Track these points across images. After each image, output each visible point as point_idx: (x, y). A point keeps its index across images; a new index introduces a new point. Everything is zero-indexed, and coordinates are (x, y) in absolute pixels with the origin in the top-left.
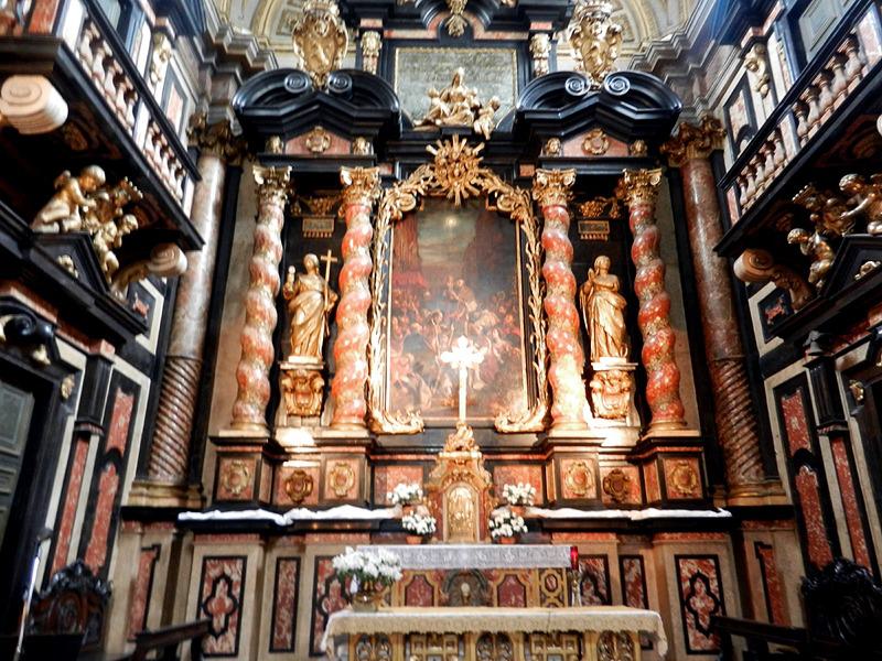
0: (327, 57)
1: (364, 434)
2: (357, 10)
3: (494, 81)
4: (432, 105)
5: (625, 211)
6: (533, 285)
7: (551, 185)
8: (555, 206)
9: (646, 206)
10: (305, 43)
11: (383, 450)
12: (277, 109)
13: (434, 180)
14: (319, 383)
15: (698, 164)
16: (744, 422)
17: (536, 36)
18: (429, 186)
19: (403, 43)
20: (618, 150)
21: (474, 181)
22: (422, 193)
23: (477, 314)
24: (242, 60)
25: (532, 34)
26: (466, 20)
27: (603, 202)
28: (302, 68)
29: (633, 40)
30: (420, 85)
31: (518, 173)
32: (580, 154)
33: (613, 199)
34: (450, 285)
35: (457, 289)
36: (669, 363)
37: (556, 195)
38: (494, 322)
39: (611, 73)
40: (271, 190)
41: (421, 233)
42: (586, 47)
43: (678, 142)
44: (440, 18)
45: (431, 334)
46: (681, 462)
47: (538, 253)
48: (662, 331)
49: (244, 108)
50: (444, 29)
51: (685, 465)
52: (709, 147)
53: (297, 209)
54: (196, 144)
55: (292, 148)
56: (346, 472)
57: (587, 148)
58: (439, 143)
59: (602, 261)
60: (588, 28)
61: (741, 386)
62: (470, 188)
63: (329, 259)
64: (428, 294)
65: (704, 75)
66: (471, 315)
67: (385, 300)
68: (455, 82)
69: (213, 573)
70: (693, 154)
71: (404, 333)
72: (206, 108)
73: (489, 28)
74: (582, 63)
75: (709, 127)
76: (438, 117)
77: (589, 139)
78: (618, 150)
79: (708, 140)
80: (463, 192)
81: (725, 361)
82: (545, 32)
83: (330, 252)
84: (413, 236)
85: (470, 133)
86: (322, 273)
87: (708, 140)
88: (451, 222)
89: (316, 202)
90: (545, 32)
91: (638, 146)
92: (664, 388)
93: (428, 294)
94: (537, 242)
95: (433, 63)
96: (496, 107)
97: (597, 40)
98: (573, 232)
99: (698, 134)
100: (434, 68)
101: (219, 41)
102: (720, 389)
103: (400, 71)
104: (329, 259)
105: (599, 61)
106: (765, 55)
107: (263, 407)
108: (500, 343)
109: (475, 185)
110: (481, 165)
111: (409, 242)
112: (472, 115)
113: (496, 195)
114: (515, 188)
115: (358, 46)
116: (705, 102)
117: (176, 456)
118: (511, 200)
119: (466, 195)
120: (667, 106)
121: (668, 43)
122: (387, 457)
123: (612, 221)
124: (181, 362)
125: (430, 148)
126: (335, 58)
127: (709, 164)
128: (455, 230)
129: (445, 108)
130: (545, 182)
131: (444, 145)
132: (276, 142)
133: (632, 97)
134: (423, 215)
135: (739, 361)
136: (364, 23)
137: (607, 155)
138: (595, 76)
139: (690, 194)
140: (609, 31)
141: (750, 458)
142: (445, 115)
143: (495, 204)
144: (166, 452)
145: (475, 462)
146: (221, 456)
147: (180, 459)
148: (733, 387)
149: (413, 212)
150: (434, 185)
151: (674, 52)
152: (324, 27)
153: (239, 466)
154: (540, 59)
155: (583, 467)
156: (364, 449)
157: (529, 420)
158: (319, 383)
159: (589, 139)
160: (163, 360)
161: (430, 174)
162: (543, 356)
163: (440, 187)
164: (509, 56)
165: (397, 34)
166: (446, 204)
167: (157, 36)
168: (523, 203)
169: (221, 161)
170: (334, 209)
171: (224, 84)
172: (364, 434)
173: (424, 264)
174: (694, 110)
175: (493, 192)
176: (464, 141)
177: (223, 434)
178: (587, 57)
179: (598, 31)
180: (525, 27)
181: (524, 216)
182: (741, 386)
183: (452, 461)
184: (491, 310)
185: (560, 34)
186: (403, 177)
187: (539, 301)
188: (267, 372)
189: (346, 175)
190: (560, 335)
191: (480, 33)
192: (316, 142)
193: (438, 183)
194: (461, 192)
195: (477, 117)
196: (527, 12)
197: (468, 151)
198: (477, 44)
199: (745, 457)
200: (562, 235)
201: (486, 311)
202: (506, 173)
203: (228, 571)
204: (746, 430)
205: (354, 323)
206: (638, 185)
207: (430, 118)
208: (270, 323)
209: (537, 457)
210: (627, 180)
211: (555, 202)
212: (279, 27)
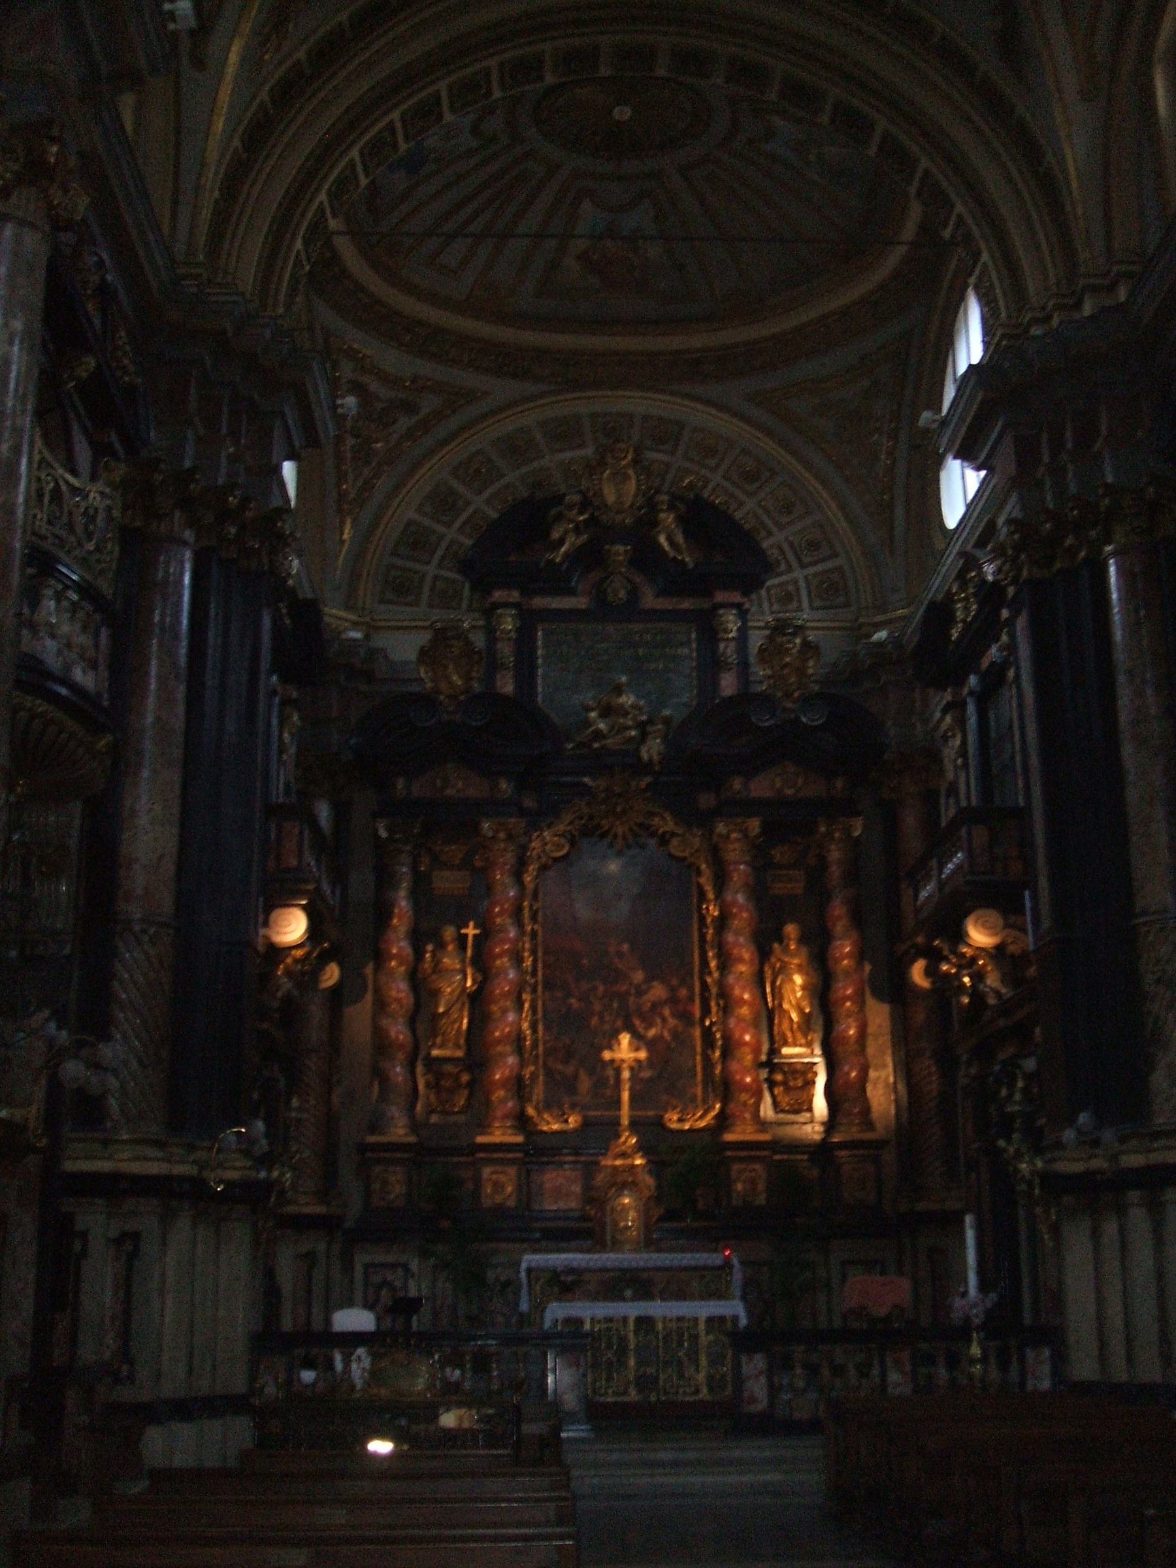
1: (520, 1139)
4: (587, 723)
14: (465, 1078)
17: (721, 611)
21: (640, 820)
26: (629, 581)
29: (849, 606)
34: (612, 949)
35: (620, 955)
56: (502, 1178)
62: (635, 828)
63: (471, 931)
66: (638, 987)
67: (534, 973)
68: (618, 690)
69: (376, 1279)
82: (732, 605)
90: (732, 605)
91: (839, 784)
98: (758, 892)
108: (672, 1022)
113: (668, 836)
132: (401, 783)
136: (498, 595)
155: (753, 1174)
157: (702, 1117)
165: (539, 602)
185: (754, 596)
201: (655, 983)
203: (390, 1278)
206: (837, 835)
211: (736, 853)
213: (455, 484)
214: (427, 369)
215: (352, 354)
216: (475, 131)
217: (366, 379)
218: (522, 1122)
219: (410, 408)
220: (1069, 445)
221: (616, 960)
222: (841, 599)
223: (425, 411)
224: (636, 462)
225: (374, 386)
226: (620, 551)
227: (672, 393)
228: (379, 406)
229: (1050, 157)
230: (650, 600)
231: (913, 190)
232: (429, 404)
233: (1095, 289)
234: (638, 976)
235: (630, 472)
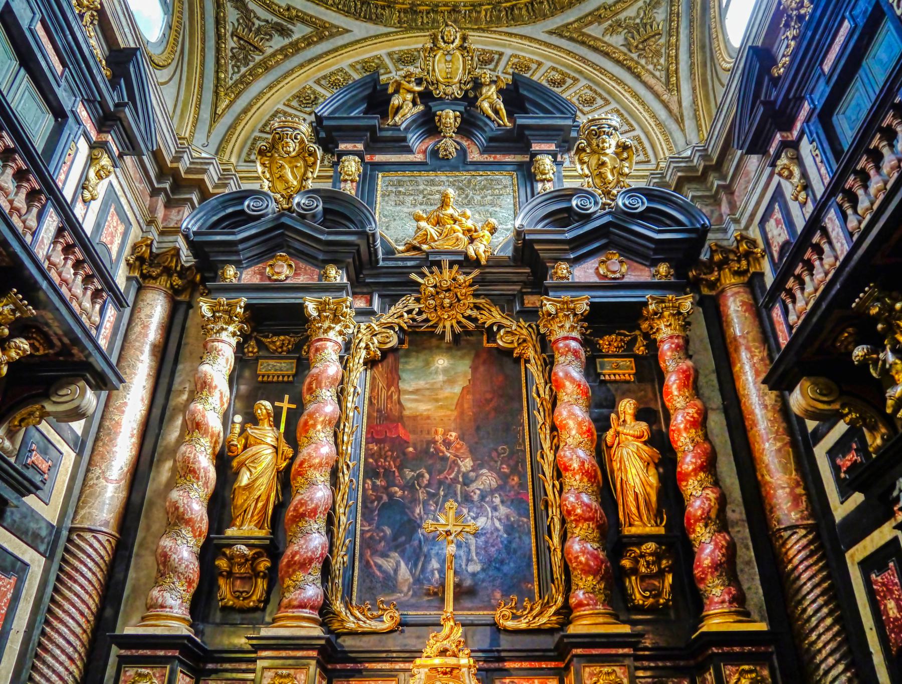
0: (295, 177)
1: (317, 631)
2: (334, 134)
3: (493, 204)
4: (419, 228)
5: (653, 345)
6: (542, 436)
7: (561, 314)
8: (566, 338)
9: (678, 337)
10: (270, 163)
11: (345, 656)
12: (233, 234)
13: (420, 313)
14: (264, 564)
15: (735, 290)
16: (825, 610)
17: (539, 157)
18: (414, 320)
19: (386, 167)
20: (643, 275)
21: (469, 312)
22: (405, 326)
23: (472, 474)
24: (200, 186)
25: (534, 155)
26: (458, 143)
27: (626, 336)
28: (266, 189)
30: (406, 210)
31: (522, 303)
32: (594, 279)
33: (637, 332)
34: (439, 438)
35: (447, 444)
36: (719, 532)
37: (567, 325)
38: (494, 484)
39: (624, 190)
40: (221, 324)
41: (404, 375)
42: (594, 161)
43: (710, 266)
44: (430, 144)
45: (415, 500)
46: (746, 667)
47: (547, 397)
48: (708, 491)
49: (195, 233)
50: (435, 153)
51: (750, 671)
52: (747, 271)
53: (252, 348)
54: (137, 274)
55: (249, 276)
57: (602, 272)
58: (425, 270)
59: (627, 406)
60: (594, 142)
61: (815, 563)
62: (464, 320)
63: (285, 405)
64: (411, 449)
65: (732, 193)
66: (465, 476)
70: (728, 279)
71: (379, 499)
72: (154, 235)
73: (485, 150)
74: (590, 180)
75: (744, 247)
76: (425, 242)
77: (603, 262)
78: (643, 275)
79: (744, 263)
80: (455, 325)
81: (793, 528)
82: (547, 153)
83: (287, 397)
84: (393, 379)
85: (461, 258)
86: (277, 425)
87: (744, 263)
88: (442, 362)
89: (275, 339)
90: (547, 153)
91: (663, 268)
92: (716, 566)
93: (411, 449)
94: (546, 383)
95: (421, 187)
96: (493, 231)
97: (605, 155)
98: (590, 369)
99: (732, 256)
100: (423, 191)
101: (175, 165)
102: (790, 567)
103: (383, 196)
104: (285, 405)
105: (610, 177)
106: (798, 160)
107: (188, 596)
108: (503, 510)
109: (469, 318)
110: (476, 296)
111: (389, 387)
112: (466, 239)
113: (495, 329)
114: (518, 321)
115: (335, 172)
116: (737, 221)
117: (67, 663)
118: (513, 334)
119: (458, 329)
120: (692, 224)
121: (689, 159)
122: (350, 666)
123: (636, 357)
124: (88, 536)
125: (414, 276)
126: (304, 178)
127: (748, 290)
128: (445, 371)
129: (432, 231)
130: (553, 310)
131: (432, 273)
132: (231, 271)
133: (647, 216)
134: (407, 354)
135: (810, 529)
137: (626, 280)
138: (607, 193)
139: (729, 324)
140: (618, 146)
141: (837, 662)
142: (432, 237)
143: (495, 341)
144: (54, 657)
145: (464, 670)
146: (123, 661)
147: (73, 668)
148: (806, 563)
149: (393, 350)
150: (419, 318)
151: (694, 169)
152: (293, 147)
153: (145, 676)
154: (543, 181)
155: (613, 677)
156: (314, 654)
157: (540, 613)
158: (264, 564)
159: (603, 262)
160: (65, 533)
161: (416, 307)
162: (558, 527)
163: (427, 320)
164: (506, 180)
165: (379, 158)
166: (434, 342)
167: (96, 152)
168: (529, 338)
169: (166, 293)
170: (298, 347)
171: (179, 211)
172: (317, 631)
173: (406, 413)
174: (725, 231)
175: (492, 326)
176: (456, 267)
177: (129, 631)
178: (596, 172)
179: (606, 145)
180: (525, 148)
181: (531, 353)
182: (815, 563)
183: (434, 669)
184: (491, 469)
185: (566, 156)
186: (383, 310)
187: (550, 456)
188: (197, 549)
189: (311, 308)
190: (578, 498)
191: (474, 155)
192: (277, 270)
193: (424, 316)
194: (452, 326)
195: (472, 240)
196: (527, 133)
197: (461, 278)
198: (471, 167)
199: (831, 661)
200: (576, 373)
201: (484, 471)
202: (505, 303)
204: (829, 621)
205: (313, 484)
206: (666, 313)
207: (415, 243)
208: (206, 484)
209: (552, 665)
210: (652, 307)
212: (249, 155)
213: (319, 89)
218: (325, 612)
219: (284, 32)
221: (443, 448)
222: (642, 158)
223: (295, 37)
224: (462, 48)
226: (449, 117)
230: (474, 155)
232: (300, 31)
234: (467, 464)
235: (458, 53)
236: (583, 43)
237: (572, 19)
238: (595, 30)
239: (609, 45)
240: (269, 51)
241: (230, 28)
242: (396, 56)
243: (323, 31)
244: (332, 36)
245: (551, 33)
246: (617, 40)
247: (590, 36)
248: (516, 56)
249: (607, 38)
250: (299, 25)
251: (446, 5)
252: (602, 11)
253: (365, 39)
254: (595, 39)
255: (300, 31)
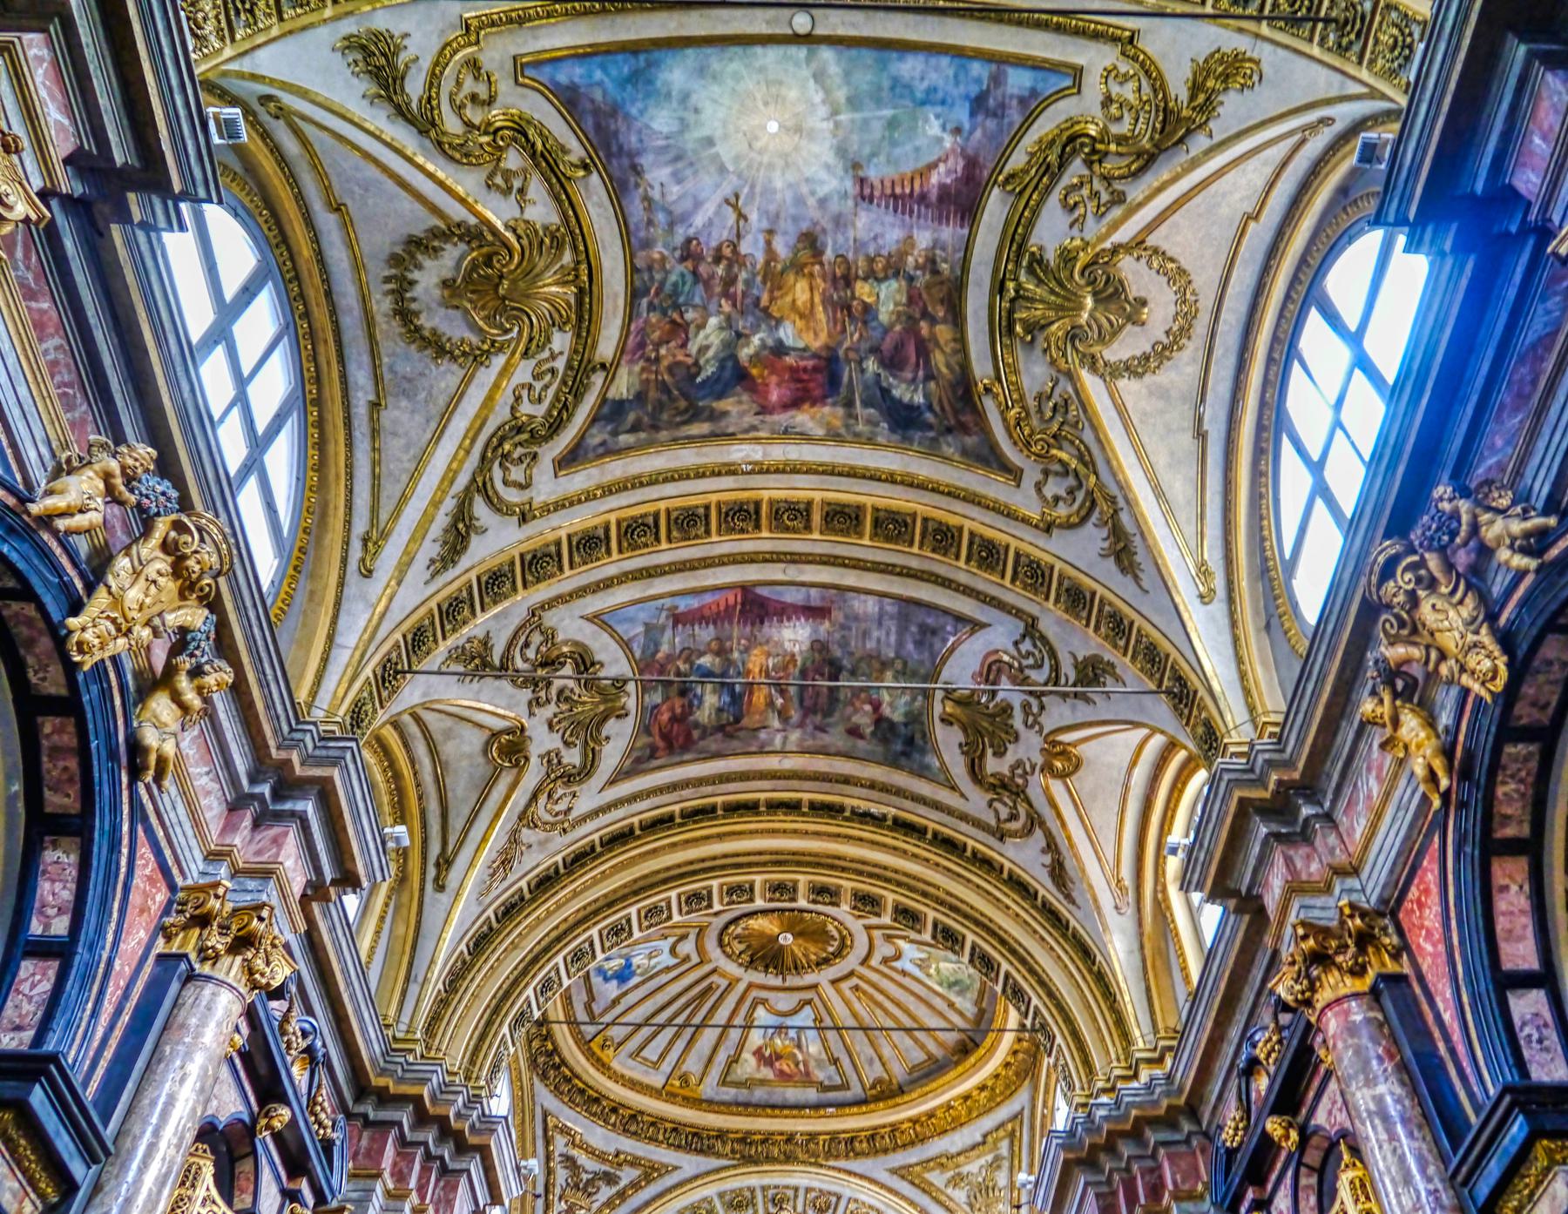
214: (628, 1145)
215: (565, 1131)
216: (673, 951)
217: (575, 1152)
219: (610, 1179)
220: (1143, 1201)
223: (623, 1183)
225: (583, 1159)
227: (834, 1168)
228: (585, 1177)
229: (1099, 958)
231: (999, 989)
232: (628, 1175)
233: (1149, 1061)
236: (924, 1190)
237: (913, 1160)
238: (937, 1178)
239: (951, 1199)
240: (596, 1206)
241: (558, 1191)
242: (727, 1198)
243: (651, 1171)
244: (660, 1175)
245: (893, 1171)
246: (960, 1195)
247: (932, 1184)
248: (856, 1201)
249: (949, 1191)
250: (626, 1168)
251: (781, 1134)
252: (944, 1160)
253: (696, 1177)
254: (938, 1190)
255: (628, 1175)
